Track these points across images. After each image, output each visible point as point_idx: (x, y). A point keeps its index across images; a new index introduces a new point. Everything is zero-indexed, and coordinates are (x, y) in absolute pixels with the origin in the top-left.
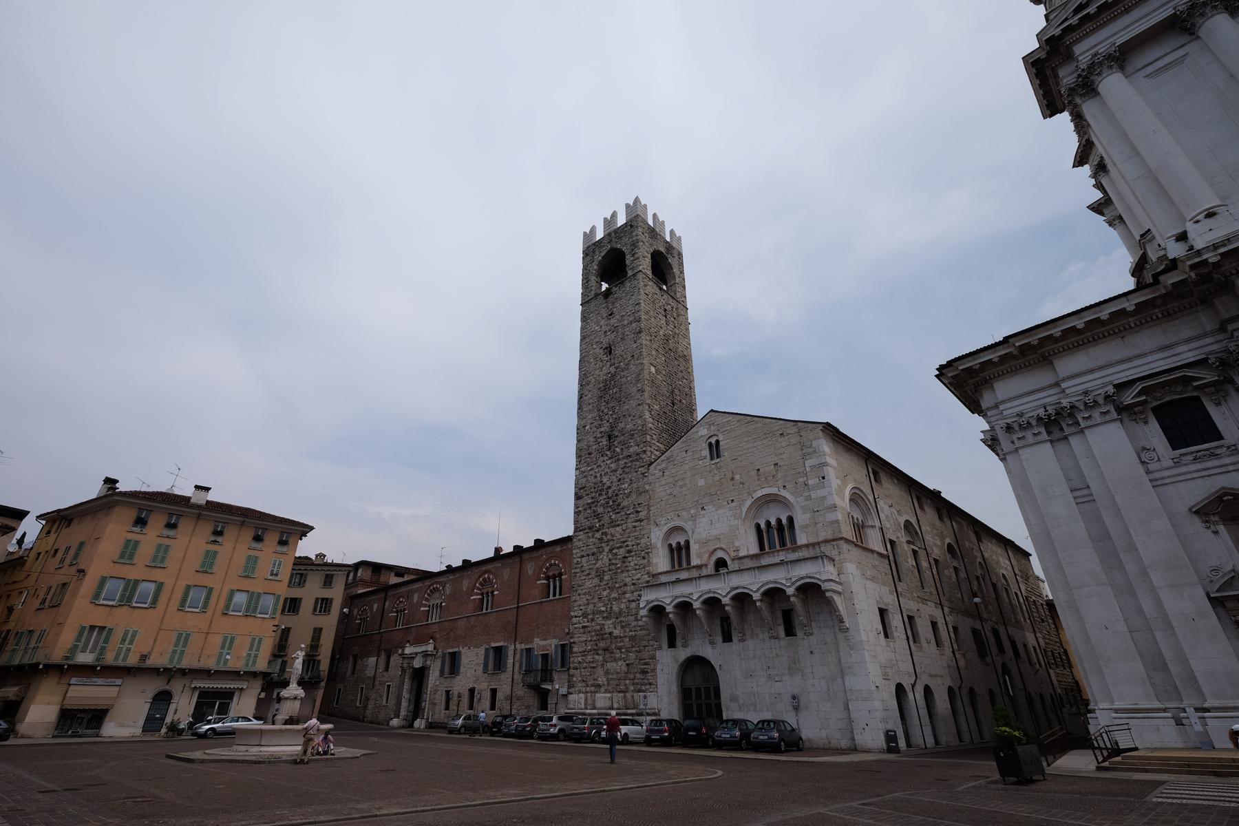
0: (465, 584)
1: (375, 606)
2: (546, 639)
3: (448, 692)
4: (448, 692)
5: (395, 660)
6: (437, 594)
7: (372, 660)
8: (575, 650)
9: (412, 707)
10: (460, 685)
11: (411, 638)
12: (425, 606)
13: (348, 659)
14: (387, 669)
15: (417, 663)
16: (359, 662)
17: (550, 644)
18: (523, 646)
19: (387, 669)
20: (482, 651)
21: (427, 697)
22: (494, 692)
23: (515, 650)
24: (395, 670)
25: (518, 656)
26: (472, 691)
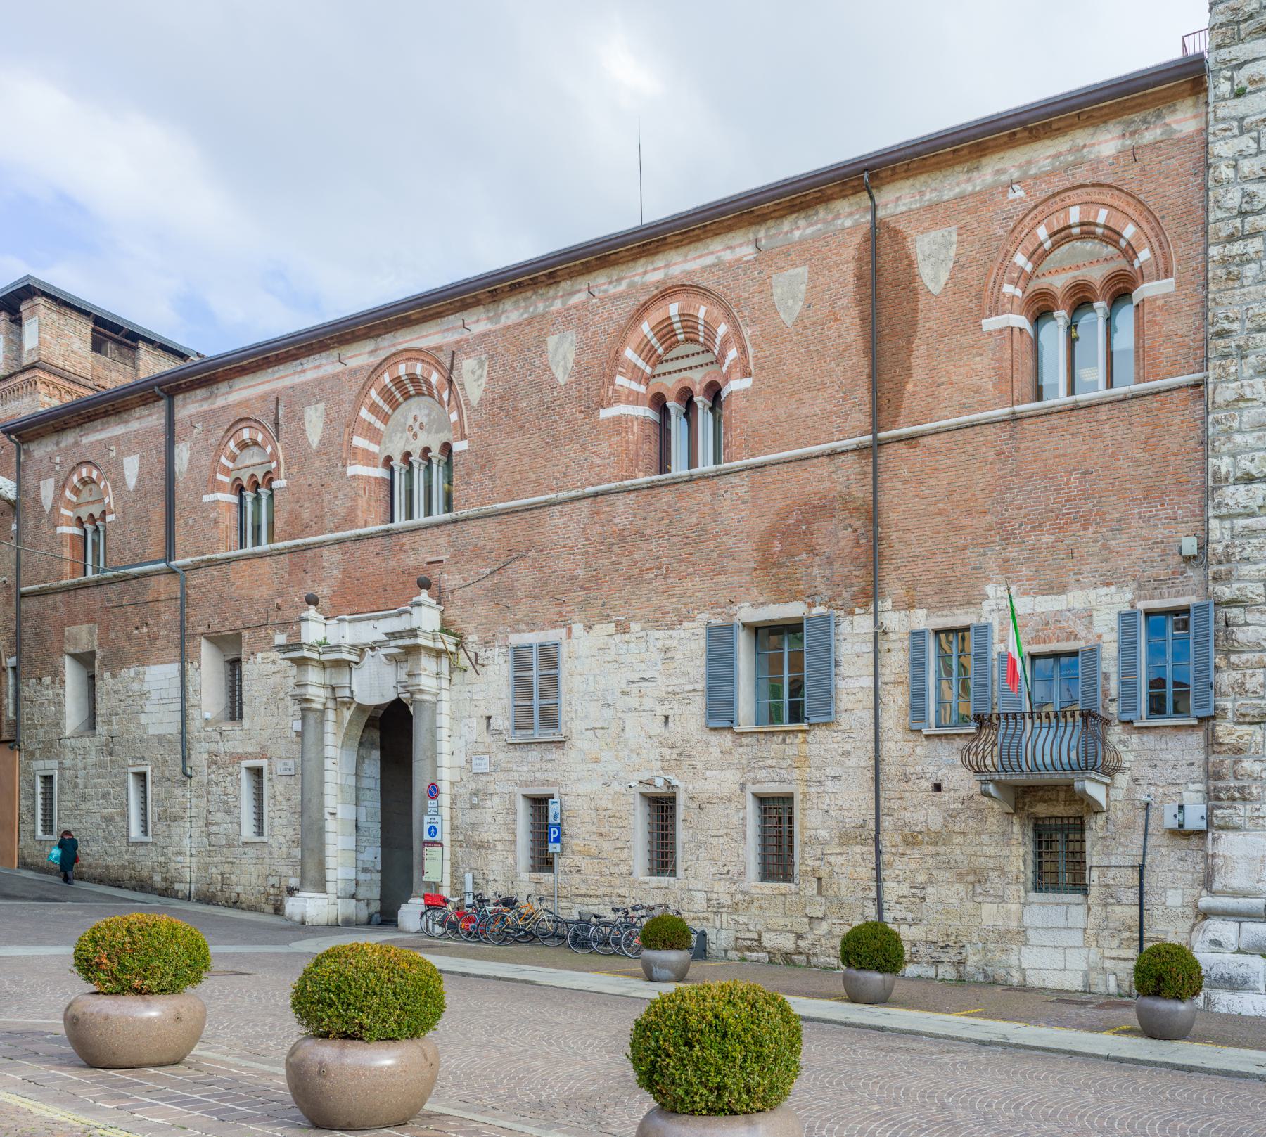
0: (562, 355)
1: (131, 467)
2: (1062, 589)
3: (539, 803)
4: (539, 803)
5: (264, 670)
6: (417, 409)
7: (160, 676)
8: (1242, 635)
9: (372, 854)
10: (597, 779)
11: (323, 591)
12: (369, 458)
13: (56, 673)
14: (235, 711)
15: (374, 685)
16: (106, 682)
17: (1096, 612)
18: (921, 620)
19: (235, 711)
20: (691, 643)
21: (437, 818)
22: (776, 813)
23: (879, 634)
24: (270, 719)
25: (896, 662)
26: (662, 807)
